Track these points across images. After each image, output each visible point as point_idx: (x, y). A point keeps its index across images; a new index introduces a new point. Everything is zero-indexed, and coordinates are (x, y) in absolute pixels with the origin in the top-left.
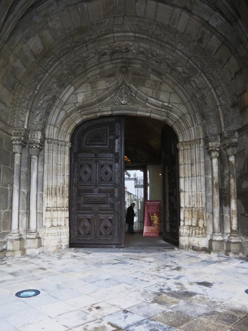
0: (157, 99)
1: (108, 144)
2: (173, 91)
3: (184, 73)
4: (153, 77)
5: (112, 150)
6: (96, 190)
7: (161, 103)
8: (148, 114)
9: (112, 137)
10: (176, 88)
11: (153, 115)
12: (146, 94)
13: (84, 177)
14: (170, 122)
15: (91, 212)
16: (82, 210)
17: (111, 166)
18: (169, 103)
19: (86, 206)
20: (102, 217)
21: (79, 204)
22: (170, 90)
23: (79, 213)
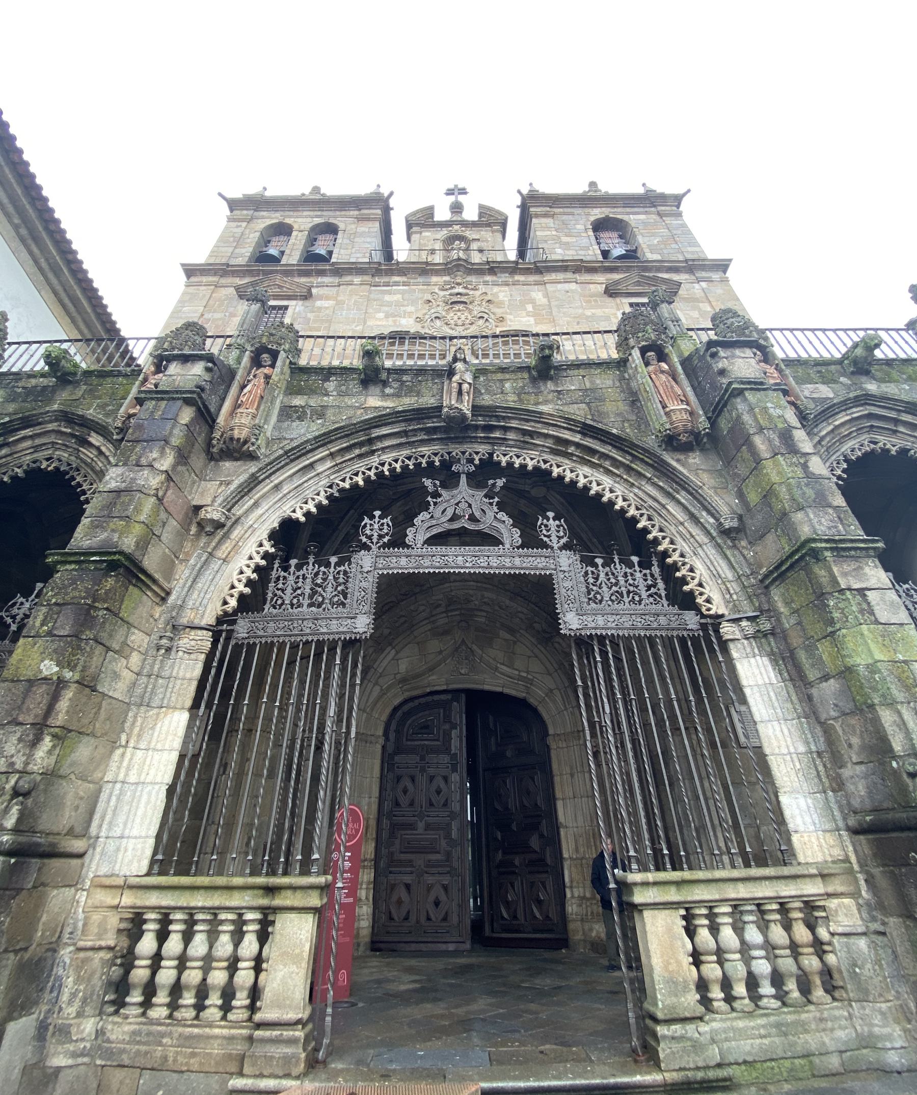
0: (511, 666)
1: (441, 739)
2: (532, 654)
3: (544, 631)
4: (504, 634)
5: (447, 750)
6: (421, 825)
7: (517, 672)
8: (499, 689)
9: (447, 727)
10: (536, 651)
11: (507, 691)
12: (494, 659)
13: (404, 801)
14: (532, 701)
15: (410, 869)
16: (396, 866)
17: (446, 779)
18: (528, 672)
19: (403, 857)
20: (430, 879)
21: (392, 854)
22: (529, 653)
23: (391, 872)
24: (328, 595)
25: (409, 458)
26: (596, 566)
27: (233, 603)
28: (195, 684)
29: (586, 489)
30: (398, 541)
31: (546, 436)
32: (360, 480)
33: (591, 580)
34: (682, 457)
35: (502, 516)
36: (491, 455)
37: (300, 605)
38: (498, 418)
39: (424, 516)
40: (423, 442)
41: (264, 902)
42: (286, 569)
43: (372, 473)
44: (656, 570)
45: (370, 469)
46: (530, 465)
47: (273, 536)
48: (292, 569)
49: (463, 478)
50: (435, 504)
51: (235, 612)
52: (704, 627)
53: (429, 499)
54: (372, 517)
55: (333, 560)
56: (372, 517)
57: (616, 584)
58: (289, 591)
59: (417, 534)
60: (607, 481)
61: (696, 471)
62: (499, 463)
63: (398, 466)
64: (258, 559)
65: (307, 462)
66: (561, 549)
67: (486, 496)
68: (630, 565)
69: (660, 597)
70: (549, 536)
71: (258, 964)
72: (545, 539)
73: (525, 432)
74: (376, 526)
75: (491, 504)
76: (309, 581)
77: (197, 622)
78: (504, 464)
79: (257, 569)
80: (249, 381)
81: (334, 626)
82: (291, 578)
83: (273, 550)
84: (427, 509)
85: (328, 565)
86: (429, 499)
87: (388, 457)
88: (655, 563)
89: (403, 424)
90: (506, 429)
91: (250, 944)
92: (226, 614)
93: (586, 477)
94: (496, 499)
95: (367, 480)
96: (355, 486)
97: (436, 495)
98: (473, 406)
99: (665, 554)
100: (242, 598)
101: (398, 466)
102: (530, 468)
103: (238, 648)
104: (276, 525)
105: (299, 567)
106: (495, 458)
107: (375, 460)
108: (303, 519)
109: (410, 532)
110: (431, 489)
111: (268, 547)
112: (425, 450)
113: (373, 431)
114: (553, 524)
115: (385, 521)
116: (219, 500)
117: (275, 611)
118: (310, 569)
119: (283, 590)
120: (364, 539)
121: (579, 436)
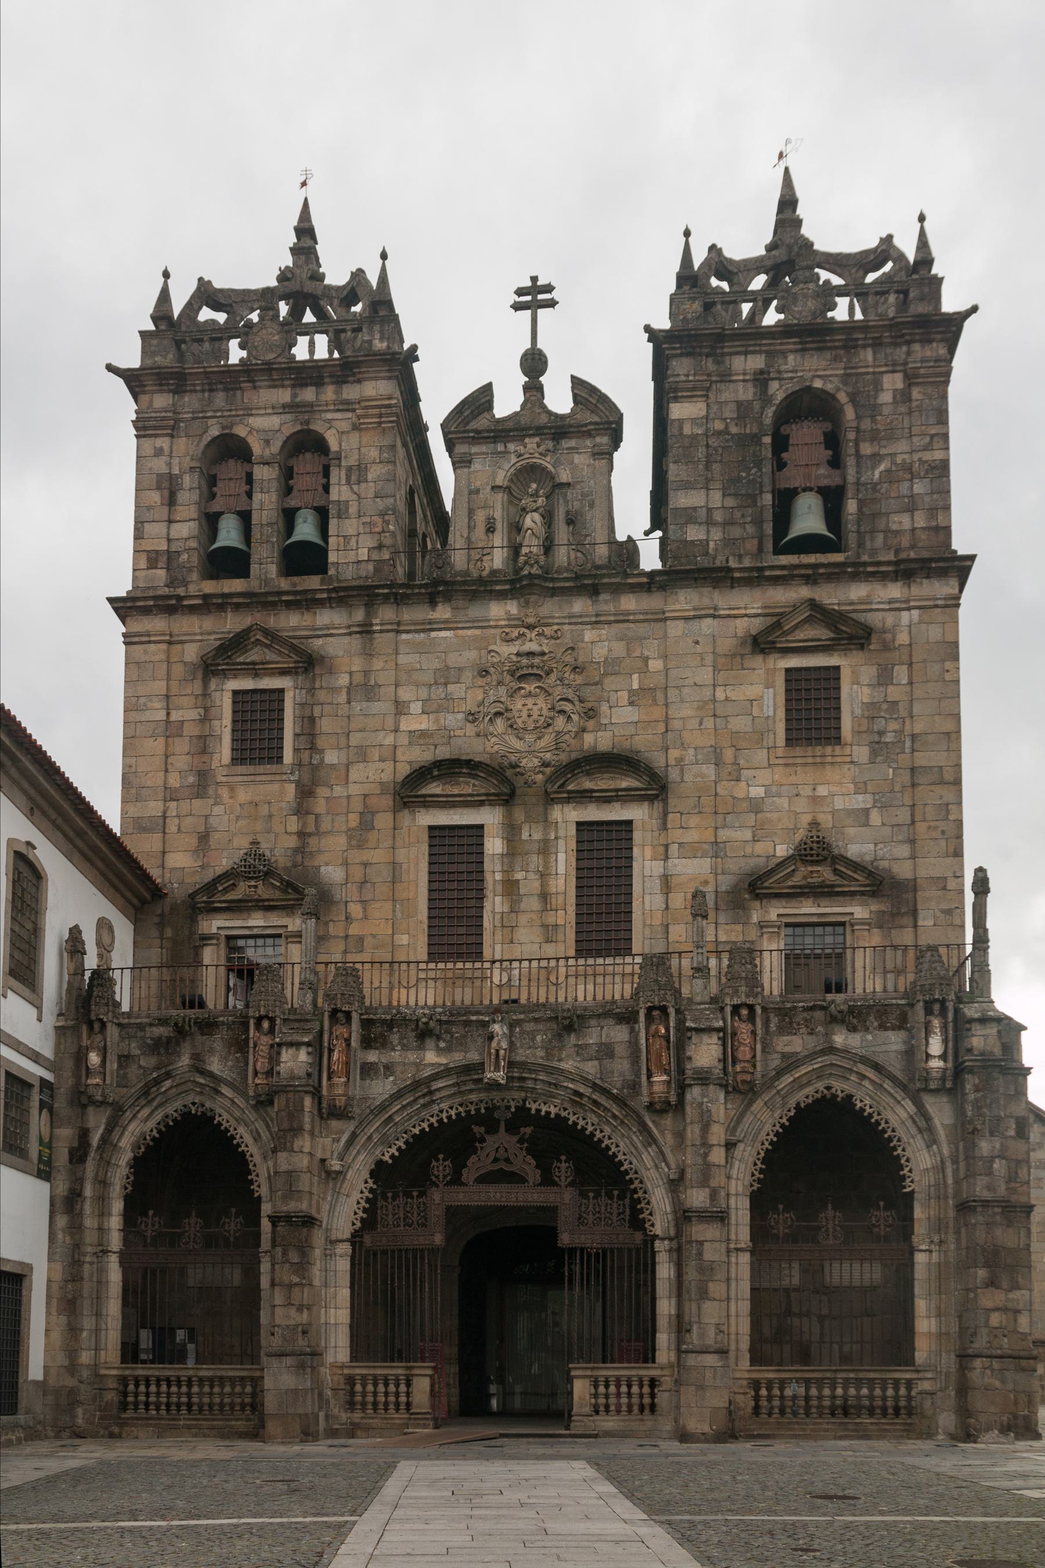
24: (415, 1219)
25: (461, 1105)
26: (588, 1198)
27: (359, 1224)
28: (348, 1274)
29: (593, 1135)
30: (456, 1180)
31: (567, 1087)
32: (425, 1125)
33: (583, 1209)
34: (657, 1119)
35: (530, 1159)
36: (524, 1101)
37: (399, 1226)
38: (530, 1071)
39: (473, 1159)
40: (471, 1091)
41: (408, 1372)
42: (386, 1199)
43: (434, 1120)
44: (627, 1201)
45: (432, 1116)
46: (553, 1111)
47: (373, 1174)
48: (390, 1200)
49: (502, 1125)
50: (482, 1148)
51: (362, 1229)
52: (645, 1242)
53: (477, 1144)
54: (437, 1160)
55: (415, 1194)
56: (437, 1160)
57: (599, 1212)
58: (390, 1216)
59: (469, 1175)
60: (608, 1130)
61: (662, 1133)
62: (530, 1109)
63: (453, 1113)
64: (367, 1194)
65: (387, 1115)
66: (566, 1186)
67: (518, 1142)
68: (611, 1198)
69: (624, 1220)
70: (559, 1177)
71: (408, 1394)
72: (557, 1179)
73: (550, 1084)
74: (441, 1168)
75: (521, 1149)
76: (401, 1208)
77: (341, 1237)
78: (533, 1112)
79: (368, 1200)
80: (334, 1046)
81: (421, 1240)
82: (390, 1207)
83: (375, 1187)
84: (475, 1153)
85: (412, 1198)
86: (477, 1144)
87: (444, 1106)
88: (628, 1196)
89: (455, 1076)
90: (536, 1080)
91: (403, 1388)
92: (356, 1231)
93: (593, 1125)
94: (526, 1145)
95: (431, 1125)
96: (423, 1131)
97: (482, 1140)
98: (509, 1062)
99: (635, 1191)
100: (362, 1220)
101: (453, 1113)
102: (552, 1116)
103: (367, 1251)
104: (373, 1166)
105: (394, 1199)
106: (528, 1105)
107: (435, 1108)
108: (390, 1161)
109: (465, 1171)
110: (478, 1136)
111: (371, 1184)
112: (473, 1097)
113: (433, 1083)
114: (564, 1165)
115: (446, 1163)
116: (336, 1154)
117: (385, 1229)
118: (401, 1200)
119: (387, 1215)
120: (434, 1179)
121: (590, 1090)
